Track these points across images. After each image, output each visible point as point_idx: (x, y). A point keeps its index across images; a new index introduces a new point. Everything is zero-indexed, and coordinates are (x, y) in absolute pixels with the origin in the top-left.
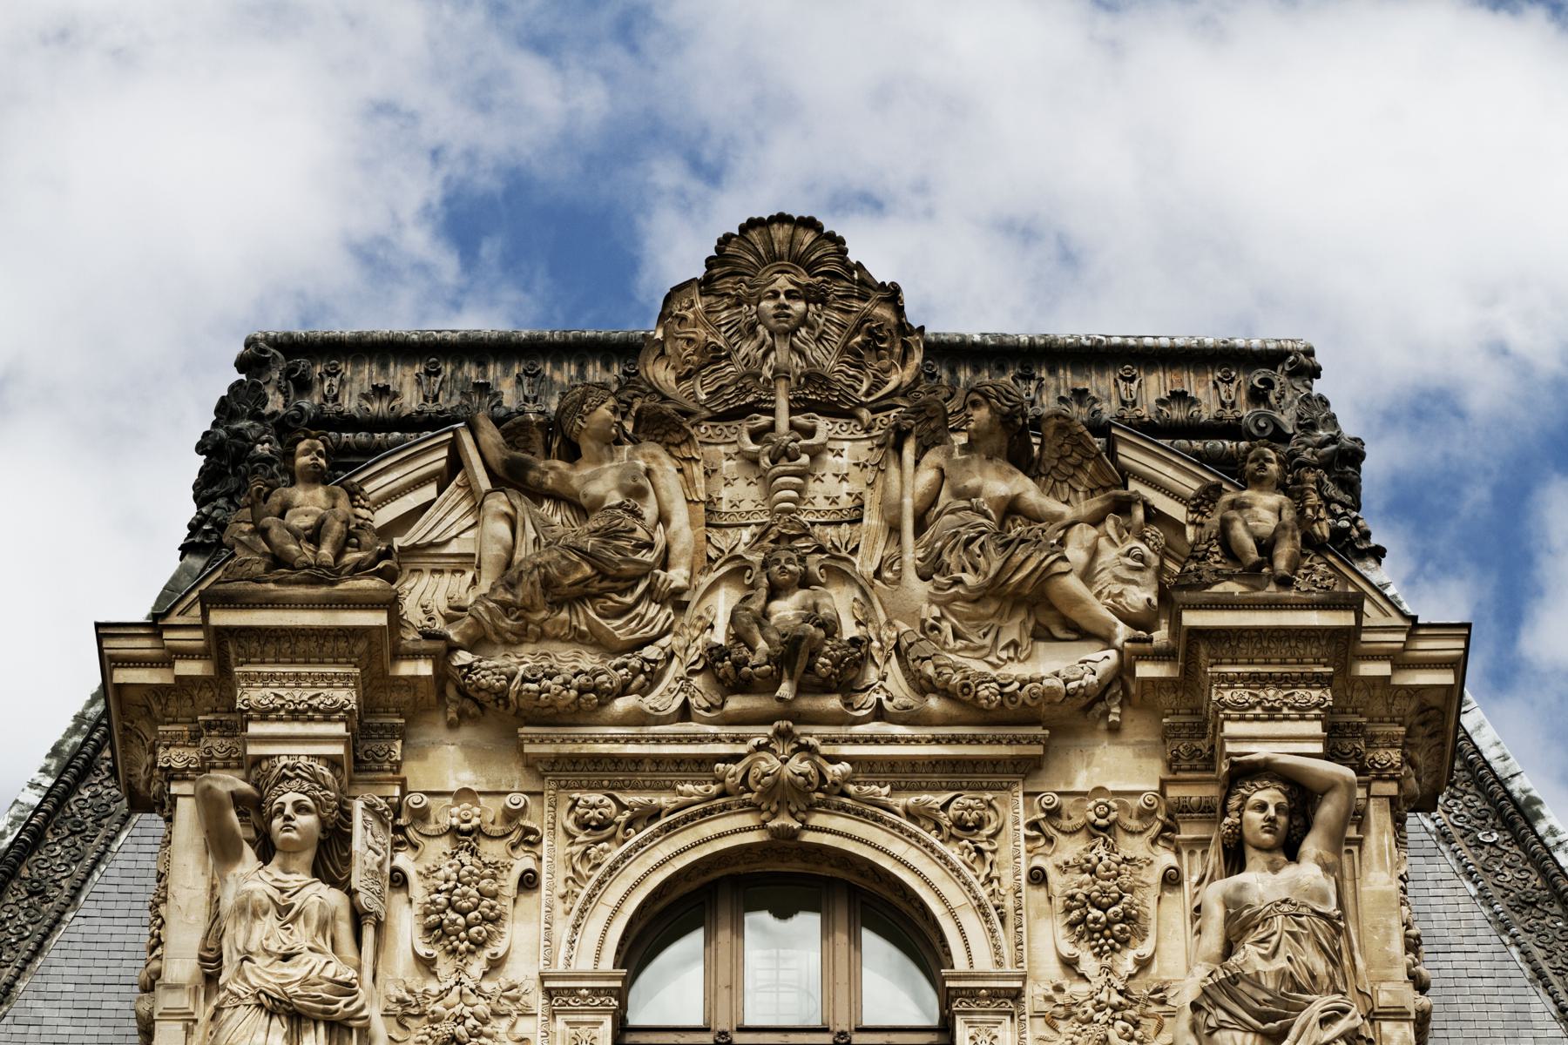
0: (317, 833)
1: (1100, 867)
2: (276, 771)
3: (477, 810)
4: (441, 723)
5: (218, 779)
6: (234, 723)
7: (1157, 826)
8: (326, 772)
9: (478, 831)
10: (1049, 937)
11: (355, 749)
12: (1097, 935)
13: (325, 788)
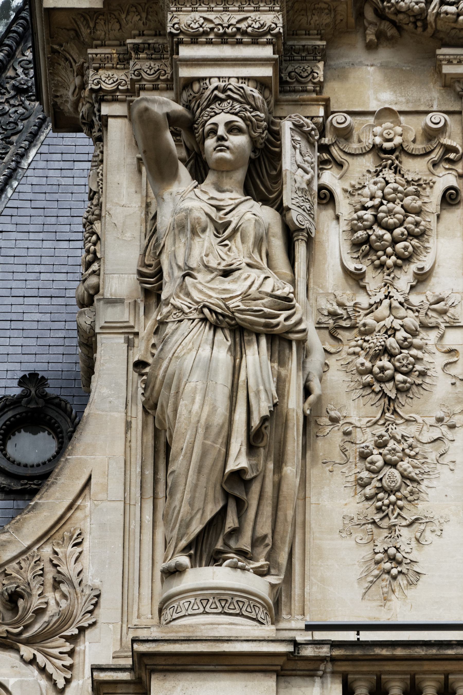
0: (248, 152)
2: (208, 93)
3: (399, 129)
4: (360, 45)
5: (154, 101)
6: (165, 46)
8: (256, 94)
9: (400, 148)
11: (281, 72)
13: (256, 109)
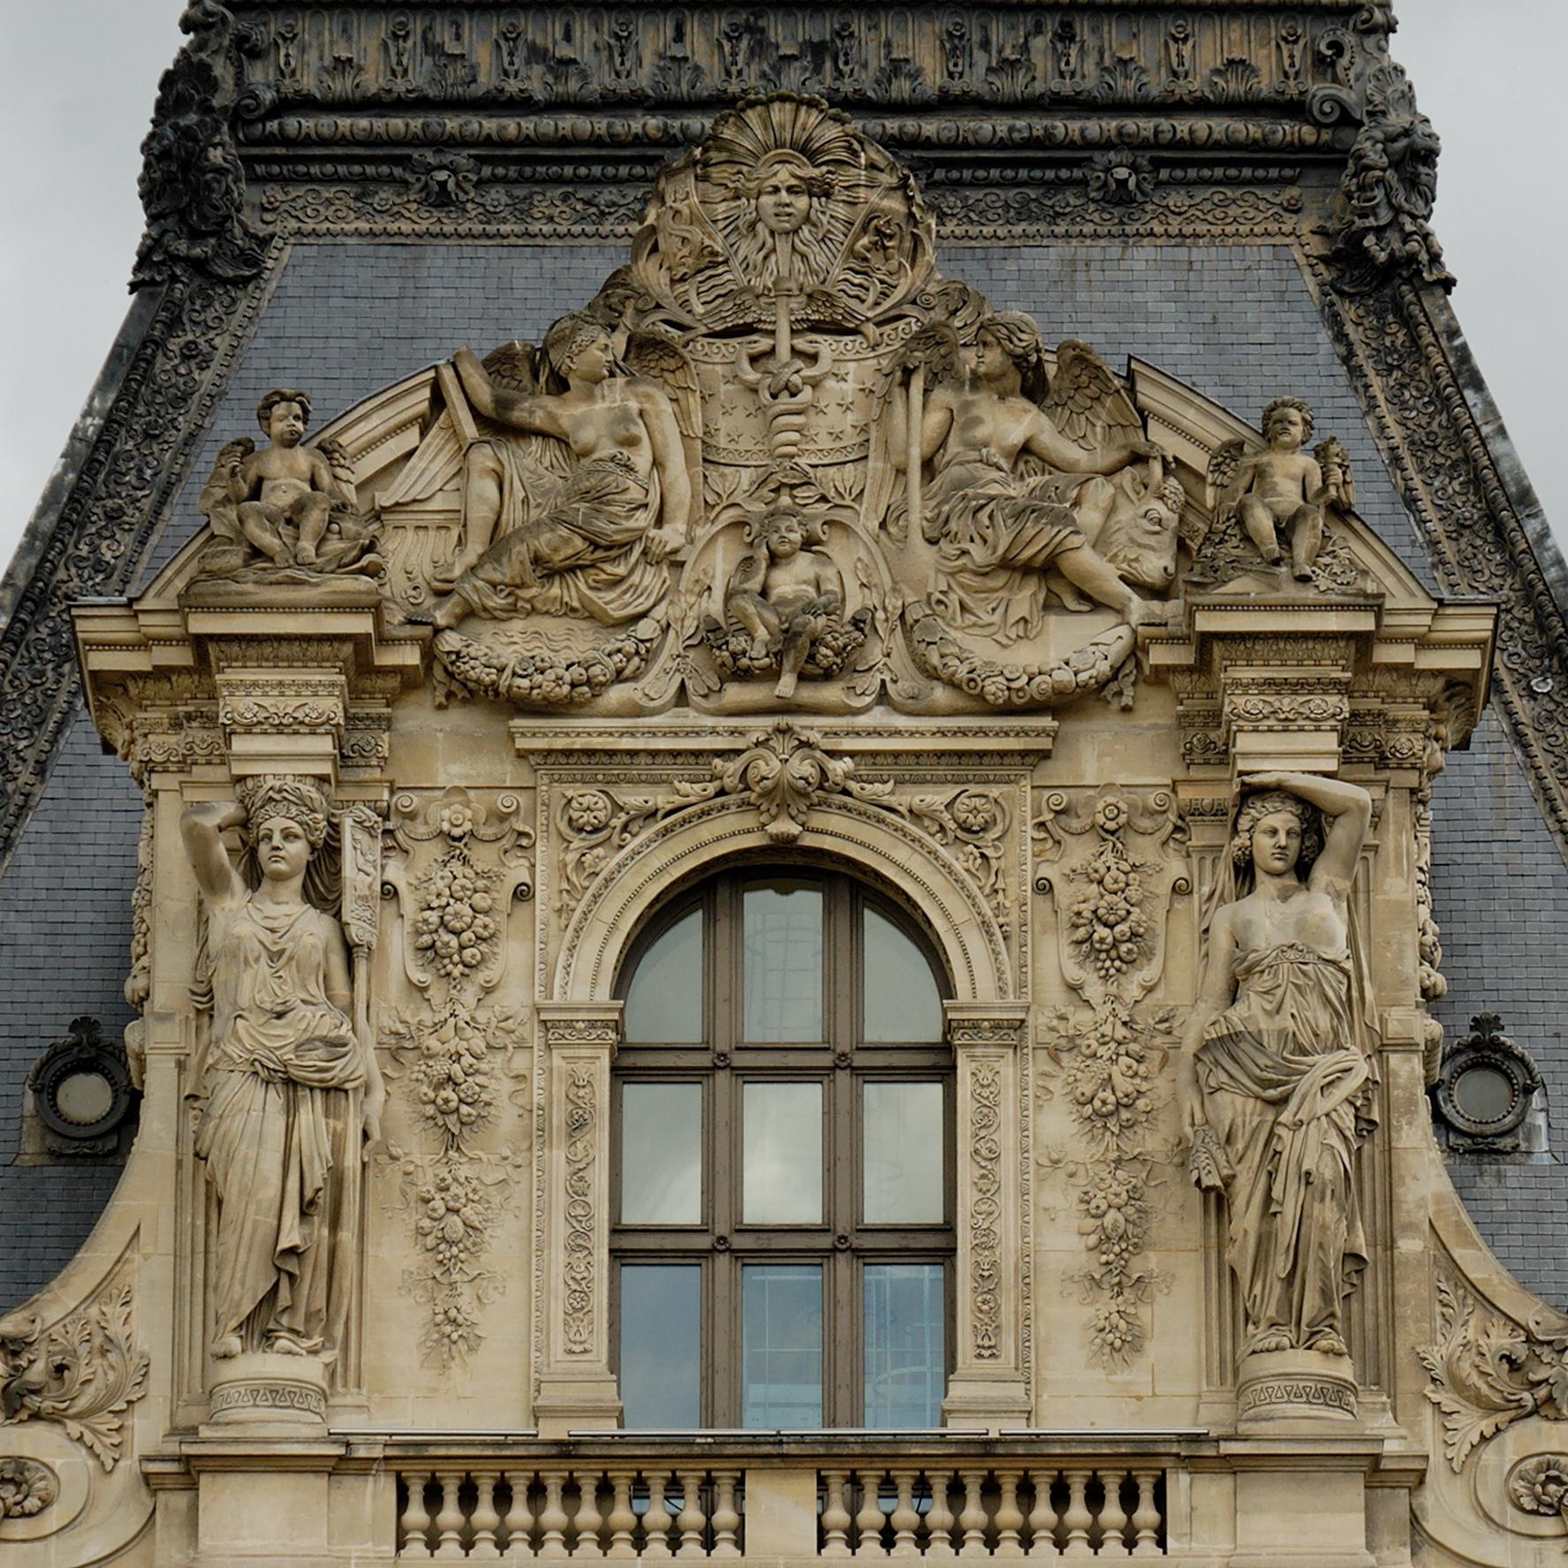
1: (1108, 880)
7: (1170, 827)
10: (1056, 958)
12: (1103, 956)
